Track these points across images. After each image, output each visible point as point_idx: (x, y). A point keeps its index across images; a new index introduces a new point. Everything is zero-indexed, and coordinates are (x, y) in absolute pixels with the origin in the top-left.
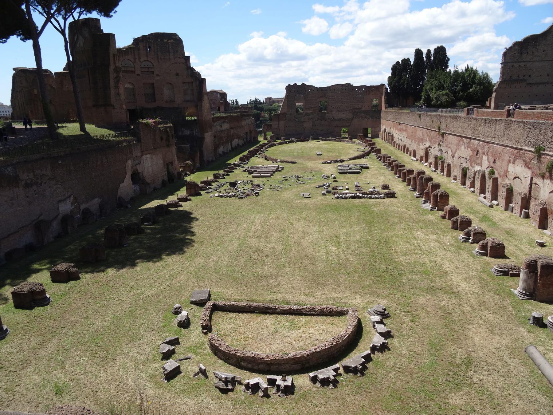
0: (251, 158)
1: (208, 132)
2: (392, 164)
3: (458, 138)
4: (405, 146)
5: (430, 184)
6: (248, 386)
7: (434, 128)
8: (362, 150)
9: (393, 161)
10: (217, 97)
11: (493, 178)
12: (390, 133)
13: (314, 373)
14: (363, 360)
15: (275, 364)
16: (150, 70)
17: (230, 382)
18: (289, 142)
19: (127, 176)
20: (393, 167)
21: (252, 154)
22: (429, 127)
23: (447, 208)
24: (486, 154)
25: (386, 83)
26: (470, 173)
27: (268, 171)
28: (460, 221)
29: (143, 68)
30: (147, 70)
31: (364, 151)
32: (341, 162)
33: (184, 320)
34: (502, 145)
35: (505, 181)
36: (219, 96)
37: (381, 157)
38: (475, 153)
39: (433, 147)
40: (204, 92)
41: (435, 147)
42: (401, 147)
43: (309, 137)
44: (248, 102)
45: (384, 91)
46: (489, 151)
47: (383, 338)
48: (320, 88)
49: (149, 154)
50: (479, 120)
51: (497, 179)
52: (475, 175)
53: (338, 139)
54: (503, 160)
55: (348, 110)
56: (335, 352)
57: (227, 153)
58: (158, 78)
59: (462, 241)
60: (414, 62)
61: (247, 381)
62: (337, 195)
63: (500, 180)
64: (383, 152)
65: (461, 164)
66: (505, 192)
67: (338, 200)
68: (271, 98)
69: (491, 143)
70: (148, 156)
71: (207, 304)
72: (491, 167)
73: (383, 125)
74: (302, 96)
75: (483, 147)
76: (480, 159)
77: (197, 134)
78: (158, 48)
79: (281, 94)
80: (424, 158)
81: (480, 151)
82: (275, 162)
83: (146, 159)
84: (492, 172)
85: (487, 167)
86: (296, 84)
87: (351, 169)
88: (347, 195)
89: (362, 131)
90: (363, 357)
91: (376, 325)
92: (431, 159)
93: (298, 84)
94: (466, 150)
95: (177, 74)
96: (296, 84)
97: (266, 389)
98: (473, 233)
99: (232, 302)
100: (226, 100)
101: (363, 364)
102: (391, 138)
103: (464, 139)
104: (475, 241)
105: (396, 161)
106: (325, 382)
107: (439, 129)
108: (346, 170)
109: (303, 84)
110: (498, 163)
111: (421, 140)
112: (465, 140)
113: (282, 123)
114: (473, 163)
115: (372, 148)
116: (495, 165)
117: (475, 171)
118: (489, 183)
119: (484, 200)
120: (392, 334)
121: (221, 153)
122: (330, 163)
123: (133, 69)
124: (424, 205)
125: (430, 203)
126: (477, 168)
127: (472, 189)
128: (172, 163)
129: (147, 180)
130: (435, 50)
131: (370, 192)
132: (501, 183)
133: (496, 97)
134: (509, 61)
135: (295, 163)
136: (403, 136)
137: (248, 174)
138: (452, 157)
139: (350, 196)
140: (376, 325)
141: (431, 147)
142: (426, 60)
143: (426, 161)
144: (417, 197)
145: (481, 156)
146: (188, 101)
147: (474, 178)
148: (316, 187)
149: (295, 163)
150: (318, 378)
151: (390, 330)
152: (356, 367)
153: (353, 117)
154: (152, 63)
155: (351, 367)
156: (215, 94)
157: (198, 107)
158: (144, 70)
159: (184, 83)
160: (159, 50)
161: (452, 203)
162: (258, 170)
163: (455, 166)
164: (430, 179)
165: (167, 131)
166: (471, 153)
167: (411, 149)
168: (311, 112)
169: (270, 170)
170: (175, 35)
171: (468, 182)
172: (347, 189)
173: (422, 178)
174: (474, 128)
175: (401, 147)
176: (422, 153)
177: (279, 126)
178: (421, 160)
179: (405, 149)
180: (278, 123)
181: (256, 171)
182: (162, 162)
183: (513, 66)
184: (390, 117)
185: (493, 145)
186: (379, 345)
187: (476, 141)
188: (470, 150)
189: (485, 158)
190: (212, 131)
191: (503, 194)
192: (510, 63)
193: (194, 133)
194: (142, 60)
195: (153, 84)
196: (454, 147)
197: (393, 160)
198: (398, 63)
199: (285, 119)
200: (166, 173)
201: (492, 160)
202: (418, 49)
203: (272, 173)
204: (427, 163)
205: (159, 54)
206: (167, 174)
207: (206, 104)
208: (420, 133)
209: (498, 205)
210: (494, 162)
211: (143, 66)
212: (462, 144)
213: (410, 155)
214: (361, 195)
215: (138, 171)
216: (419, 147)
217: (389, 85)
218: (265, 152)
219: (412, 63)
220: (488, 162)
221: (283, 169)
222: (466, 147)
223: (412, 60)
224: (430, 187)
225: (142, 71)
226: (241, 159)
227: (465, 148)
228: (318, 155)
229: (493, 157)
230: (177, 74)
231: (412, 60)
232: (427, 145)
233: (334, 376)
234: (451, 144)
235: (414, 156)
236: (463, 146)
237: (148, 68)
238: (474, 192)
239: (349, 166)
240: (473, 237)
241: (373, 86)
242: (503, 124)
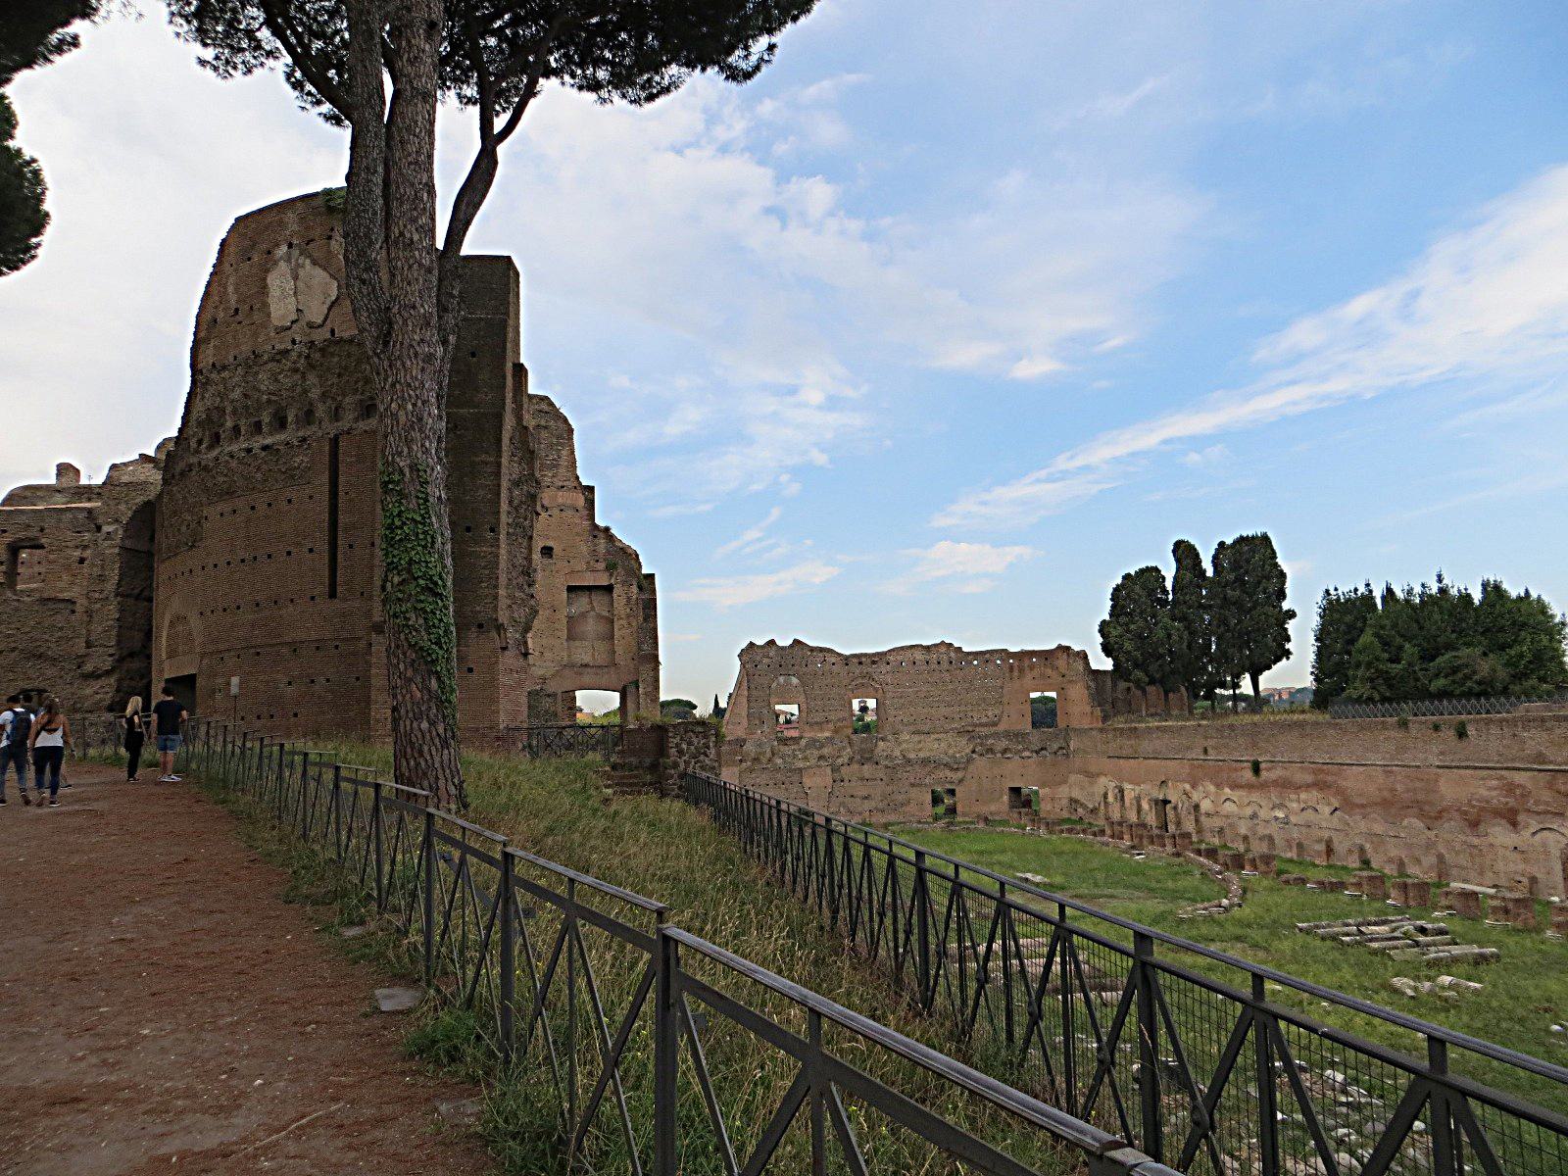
12: (1166, 802)
55: (952, 729)
73: (1092, 776)
74: (795, 681)
86: (772, 642)
89: (1006, 798)
93: (780, 643)
96: (772, 642)
109: (797, 642)
153: (973, 752)
159: (571, 589)
216: (1476, 841)
217: (1107, 649)
219: (1169, 585)
223: (1169, 571)
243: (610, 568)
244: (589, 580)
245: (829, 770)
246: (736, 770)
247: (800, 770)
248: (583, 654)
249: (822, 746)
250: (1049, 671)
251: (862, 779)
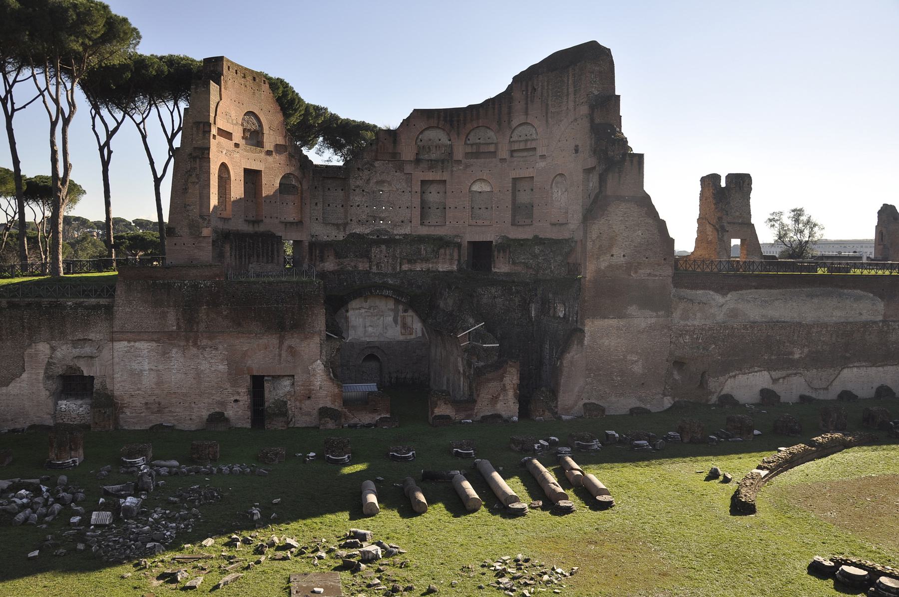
19: (24, 376)
29: (517, 141)
58: (542, 164)
123: (492, 148)
154: (536, 130)
158: (516, 147)
182: (223, 367)
194: (515, 123)
195: (533, 177)
200: (245, 398)
205: (550, 103)
211: (515, 138)
215: (83, 373)
225: (512, 152)
237: (526, 141)
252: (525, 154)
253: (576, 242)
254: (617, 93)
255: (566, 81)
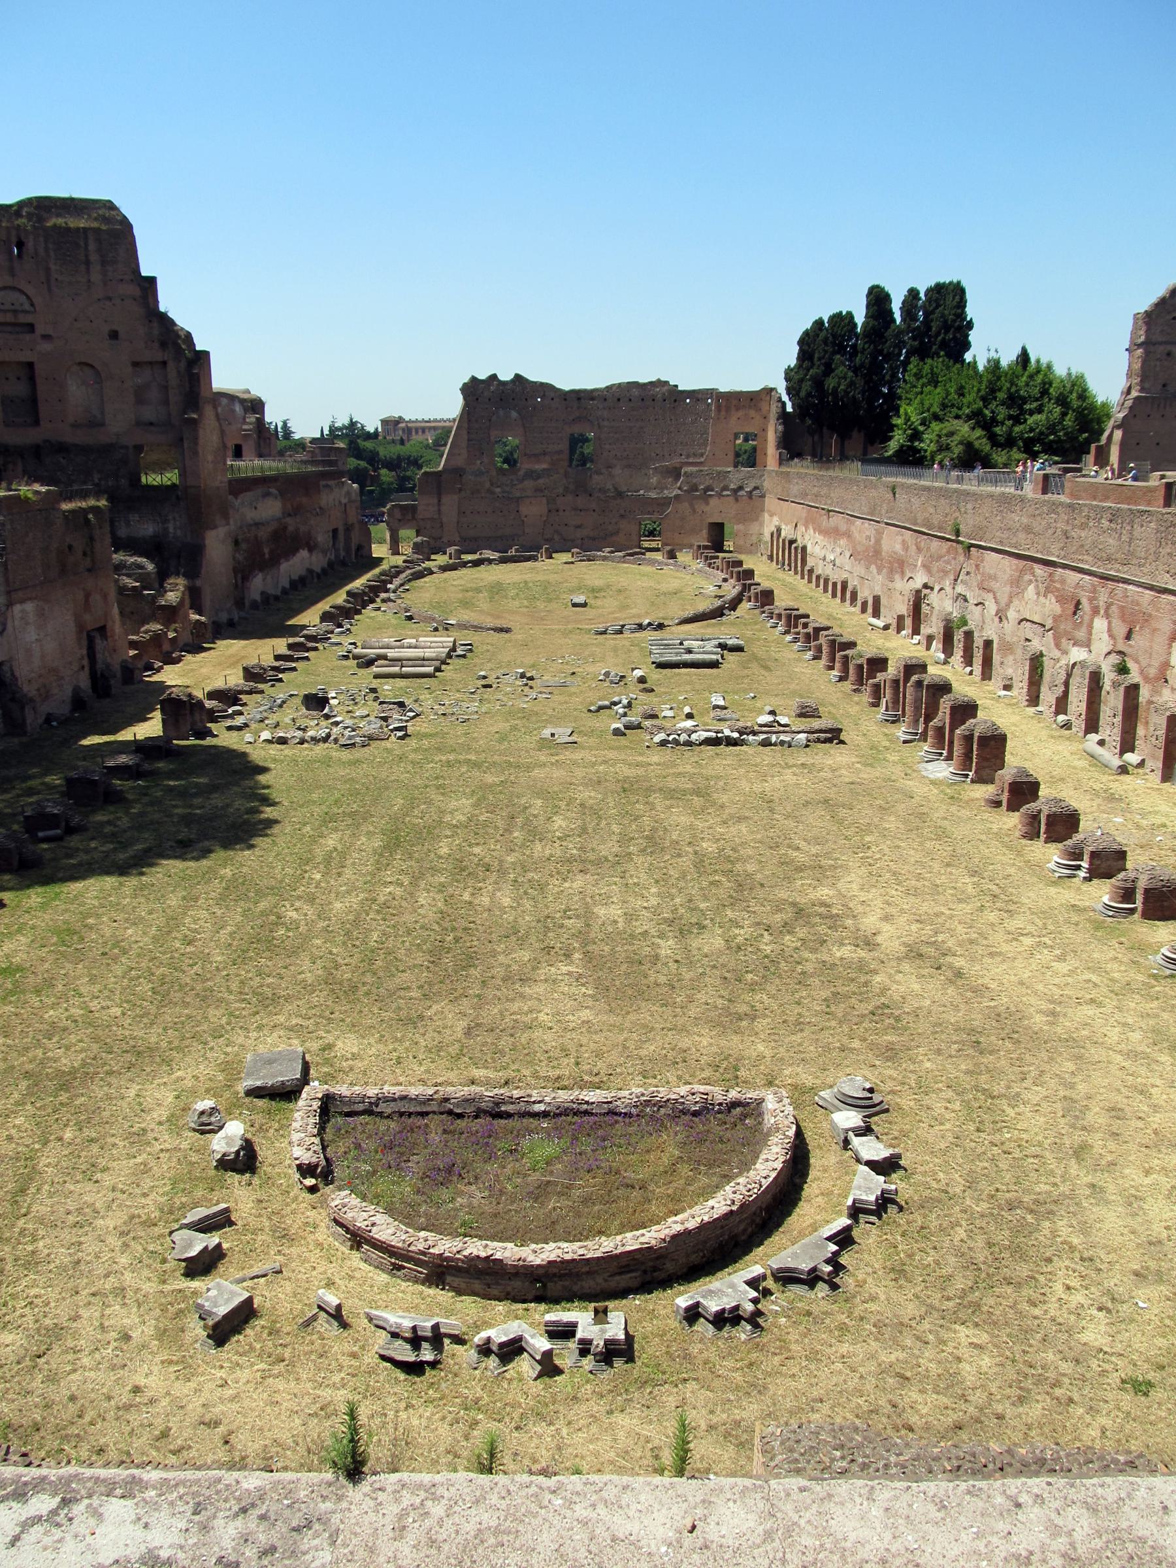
0: (359, 612)
1: (215, 527)
2: (816, 638)
3: (1015, 561)
4: (844, 585)
5: (945, 704)
6: (485, 1350)
7: (940, 529)
8: (713, 594)
9: (817, 630)
10: (233, 411)
11: (1127, 684)
13: (692, 1298)
14: (834, 1248)
15: (561, 1277)
16: (23, 319)
17: (426, 1339)
18: (477, 563)
20: (819, 649)
21: (361, 601)
22: (923, 526)
23: (1006, 774)
24: (1102, 612)
25: (781, 387)
26: (1053, 672)
27: (424, 659)
28: (1048, 816)
30: (9, 318)
31: (721, 597)
32: (655, 629)
33: (238, 1153)
34: (1151, 588)
35: (1161, 695)
36: (238, 408)
37: (779, 616)
38: (1072, 608)
39: (937, 588)
40: (204, 393)
41: (941, 589)
42: (835, 584)
43: (538, 548)
44: (326, 432)
45: (774, 409)
46: (1112, 604)
47: (882, 1178)
48: (573, 392)
49: (30, 599)
50: (1081, 511)
51: (1136, 687)
52: (1069, 675)
53: (631, 555)
54: (1155, 630)
56: (742, 1227)
57: (277, 598)
58: (46, 347)
59: (1057, 875)
60: (865, 325)
61: (484, 1334)
62: (661, 736)
63: (1144, 694)
64: (782, 601)
65: (1027, 640)
66: (1164, 727)
67: (667, 754)
68: (400, 417)
69: (1118, 581)
70: (29, 607)
71: (304, 1095)
72: (1120, 653)
73: (771, 516)
74: (514, 414)
75: (1094, 591)
76: (1084, 629)
77: (179, 533)
78: (51, 246)
79: (450, 407)
80: (908, 622)
81: (1085, 603)
82: (440, 628)
83: (22, 618)
84: (1123, 670)
85: (1106, 650)
86: (494, 377)
87: (689, 651)
88: (694, 737)
89: (705, 532)
90: (829, 1239)
91: (856, 1141)
92: (932, 627)
94: (1042, 599)
95: (114, 335)
96: (494, 377)
97: (548, 1354)
98: (1090, 849)
99: (386, 1088)
100: (261, 422)
101: (833, 1260)
102: (799, 556)
103: (1035, 566)
104: (1096, 873)
105: (827, 629)
106: (725, 1319)
107: (958, 533)
108: (677, 654)
109: (518, 377)
110: (1138, 640)
111: (898, 566)
112: (1039, 570)
113: (450, 502)
114: (1063, 640)
115: (746, 588)
116: (1130, 646)
117: (1072, 662)
118: (1112, 704)
119: (1099, 750)
120: (902, 1163)
121: (258, 597)
122: (620, 632)
124: (930, 766)
125: (949, 758)
126: (1077, 654)
127: (1061, 718)
128: (102, 630)
129: (26, 689)
130: (929, 291)
131: (761, 726)
132: (1150, 702)
133: (1123, 445)
134: (1160, 340)
135: (507, 630)
136: (838, 550)
137: (359, 666)
138: (997, 619)
139: (702, 738)
140: (856, 1141)
141: (932, 589)
142: (903, 320)
143: (916, 631)
144: (905, 742)
145: (1086, 618)
146: (151, 424)
147: (1067, 684)
148: (590, 711)
149: (507, 630)
150: (705, 1308)
151: (897, 1150)
152: (814, 1269)
155: (801, 1272)
156: (224, 401)
157: (186, 445)
159: (136, 364)
160: (52, 253)
161: (1015, 759)
162: (391, 653)
163: (1008, 648)
164: (944, 688)
165: (87, 521)
166: (1057, 609)
167: (865, 594)
168: (545, 466)
169: (429, 653)
170: (110, 206)
171: (1048, 697)
172: (690, 716)
173: (919, 684)
174: (1065, 533)
175: (835, 584)
176: (903, 608)
177: (439, 510)
178: (900, 628)
179: (843, 591)
180: (436, 501)
181: (384, 657)
182: (72, 626)
183: (1169, 354)
184: (795, 488)
185: (1125, 586)
186: (872, 1198)
187: (1071, 573)
188: (1053, 600)
189: (1100, 624)
190: (228, 524)
191: (1158, 733)
192: (1161, 343)
193: (171, 530)
195: (30, 365)
196: (1004, 591)
197: (817, 625)
198: (819, 323)
199: (460, 490)
200: (86, 662)
201: (1121, 630)
202: (878, 287)
203: (437, 663)
204: (917, 638)
205: (53, 267)
206: (87, 669)
207: (209, 435)
208: (894, 542)
209: (1141, 764)
210: (1128, 637)
212: (1031, 581)
213: (864, 610)
214: (736, 735)
216: (891, 585)
218: (403, 595)
220: (1111, 636)
221: (471, 651)
222: (1042, 590)
223: (860, 319)
224: (948, 711)
226: (325, 617)
227: (1038, 594)
228: (575, 605)
229: (1124, 621)
230: (114, 335)
231: (860, 319)
232: (920, 579)
233: (755, 1301)
234: (994, 578)
235: (876, 613)
236: (1031, 588)
237: (15, 312)
238: (1067, 726)
239: (681, 644)
240: (1091, 864)
241: (741, 392)
242: (1152, 525)
243: (163, 345)
244: (148, 356)
245: (544, 500)
246: (456, 497)
247: (518, 498)
248: (149, 413)
249: (539, 477)
250: (752, 413)
251: (575, 509)
252: (9, 329)
253: (126, 447)
254: (144, 273)
255: (82, 243)
